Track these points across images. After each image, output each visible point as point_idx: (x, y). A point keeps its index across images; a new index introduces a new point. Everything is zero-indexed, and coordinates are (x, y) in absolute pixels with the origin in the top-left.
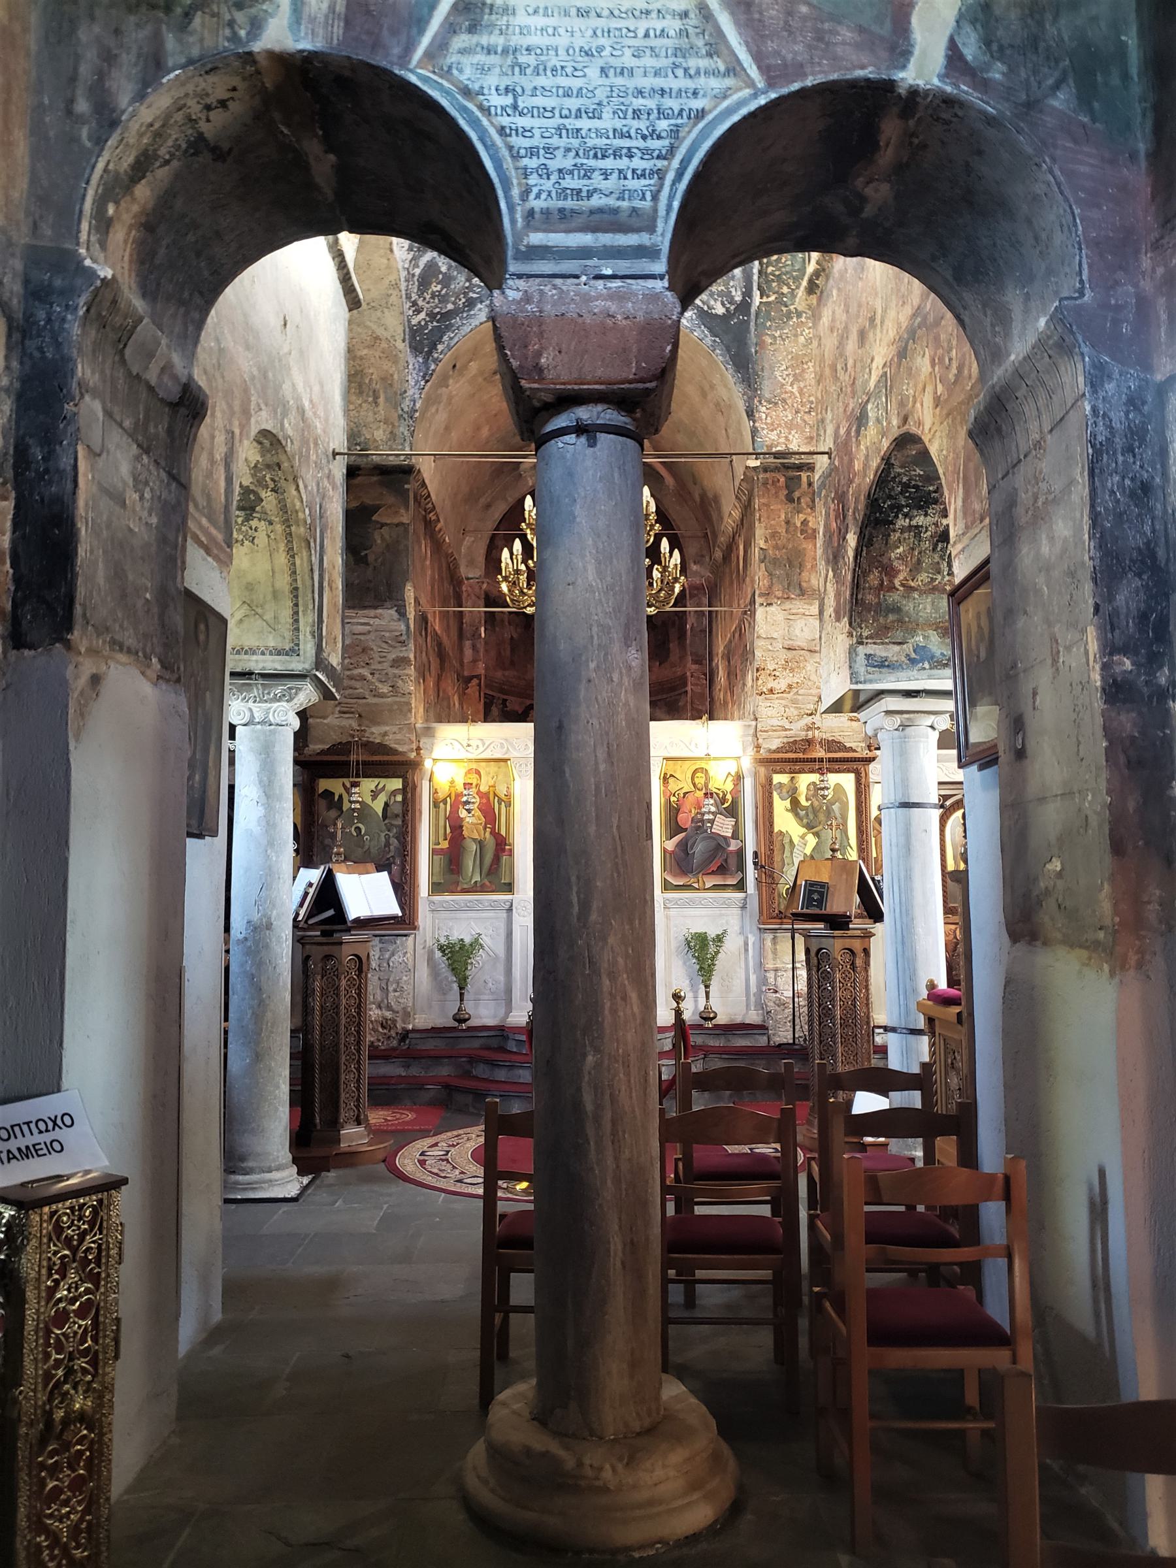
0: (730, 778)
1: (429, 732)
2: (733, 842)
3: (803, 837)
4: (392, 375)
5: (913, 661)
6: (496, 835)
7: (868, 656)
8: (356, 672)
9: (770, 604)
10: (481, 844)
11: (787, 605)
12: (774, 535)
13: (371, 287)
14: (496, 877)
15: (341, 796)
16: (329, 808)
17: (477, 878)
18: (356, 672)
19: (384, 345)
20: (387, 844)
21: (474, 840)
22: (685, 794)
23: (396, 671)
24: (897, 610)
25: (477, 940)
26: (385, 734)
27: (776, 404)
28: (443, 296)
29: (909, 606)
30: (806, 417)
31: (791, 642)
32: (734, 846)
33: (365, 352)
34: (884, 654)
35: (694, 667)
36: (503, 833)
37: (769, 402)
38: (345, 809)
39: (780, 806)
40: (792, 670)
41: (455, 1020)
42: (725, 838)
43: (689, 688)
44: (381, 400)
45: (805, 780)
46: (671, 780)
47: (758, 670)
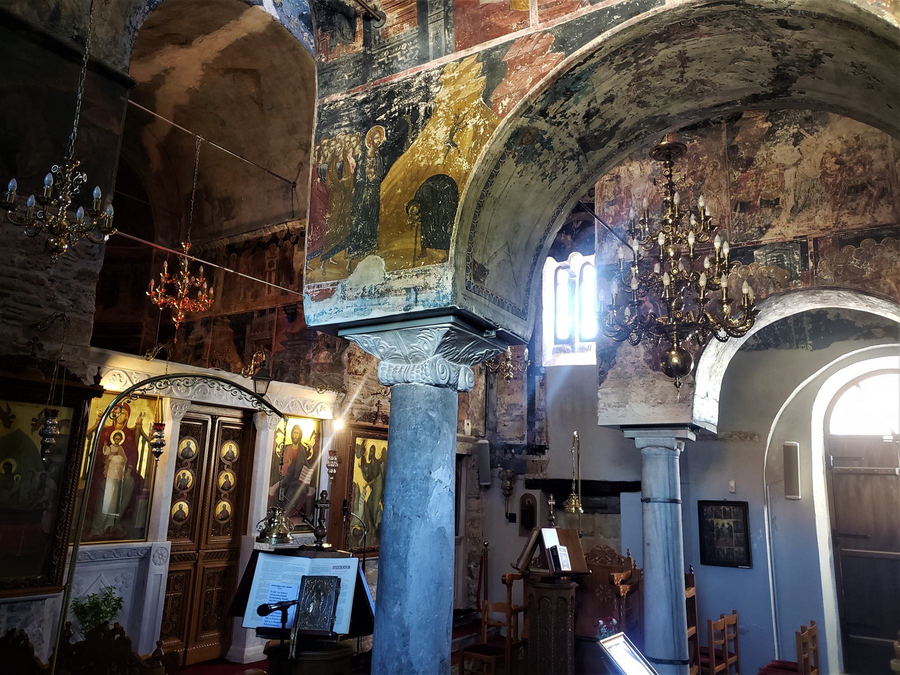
8: (33, 273)
18: (33, 273)
23: (80, 284)
26: (58, 352)
47: (349, 355)
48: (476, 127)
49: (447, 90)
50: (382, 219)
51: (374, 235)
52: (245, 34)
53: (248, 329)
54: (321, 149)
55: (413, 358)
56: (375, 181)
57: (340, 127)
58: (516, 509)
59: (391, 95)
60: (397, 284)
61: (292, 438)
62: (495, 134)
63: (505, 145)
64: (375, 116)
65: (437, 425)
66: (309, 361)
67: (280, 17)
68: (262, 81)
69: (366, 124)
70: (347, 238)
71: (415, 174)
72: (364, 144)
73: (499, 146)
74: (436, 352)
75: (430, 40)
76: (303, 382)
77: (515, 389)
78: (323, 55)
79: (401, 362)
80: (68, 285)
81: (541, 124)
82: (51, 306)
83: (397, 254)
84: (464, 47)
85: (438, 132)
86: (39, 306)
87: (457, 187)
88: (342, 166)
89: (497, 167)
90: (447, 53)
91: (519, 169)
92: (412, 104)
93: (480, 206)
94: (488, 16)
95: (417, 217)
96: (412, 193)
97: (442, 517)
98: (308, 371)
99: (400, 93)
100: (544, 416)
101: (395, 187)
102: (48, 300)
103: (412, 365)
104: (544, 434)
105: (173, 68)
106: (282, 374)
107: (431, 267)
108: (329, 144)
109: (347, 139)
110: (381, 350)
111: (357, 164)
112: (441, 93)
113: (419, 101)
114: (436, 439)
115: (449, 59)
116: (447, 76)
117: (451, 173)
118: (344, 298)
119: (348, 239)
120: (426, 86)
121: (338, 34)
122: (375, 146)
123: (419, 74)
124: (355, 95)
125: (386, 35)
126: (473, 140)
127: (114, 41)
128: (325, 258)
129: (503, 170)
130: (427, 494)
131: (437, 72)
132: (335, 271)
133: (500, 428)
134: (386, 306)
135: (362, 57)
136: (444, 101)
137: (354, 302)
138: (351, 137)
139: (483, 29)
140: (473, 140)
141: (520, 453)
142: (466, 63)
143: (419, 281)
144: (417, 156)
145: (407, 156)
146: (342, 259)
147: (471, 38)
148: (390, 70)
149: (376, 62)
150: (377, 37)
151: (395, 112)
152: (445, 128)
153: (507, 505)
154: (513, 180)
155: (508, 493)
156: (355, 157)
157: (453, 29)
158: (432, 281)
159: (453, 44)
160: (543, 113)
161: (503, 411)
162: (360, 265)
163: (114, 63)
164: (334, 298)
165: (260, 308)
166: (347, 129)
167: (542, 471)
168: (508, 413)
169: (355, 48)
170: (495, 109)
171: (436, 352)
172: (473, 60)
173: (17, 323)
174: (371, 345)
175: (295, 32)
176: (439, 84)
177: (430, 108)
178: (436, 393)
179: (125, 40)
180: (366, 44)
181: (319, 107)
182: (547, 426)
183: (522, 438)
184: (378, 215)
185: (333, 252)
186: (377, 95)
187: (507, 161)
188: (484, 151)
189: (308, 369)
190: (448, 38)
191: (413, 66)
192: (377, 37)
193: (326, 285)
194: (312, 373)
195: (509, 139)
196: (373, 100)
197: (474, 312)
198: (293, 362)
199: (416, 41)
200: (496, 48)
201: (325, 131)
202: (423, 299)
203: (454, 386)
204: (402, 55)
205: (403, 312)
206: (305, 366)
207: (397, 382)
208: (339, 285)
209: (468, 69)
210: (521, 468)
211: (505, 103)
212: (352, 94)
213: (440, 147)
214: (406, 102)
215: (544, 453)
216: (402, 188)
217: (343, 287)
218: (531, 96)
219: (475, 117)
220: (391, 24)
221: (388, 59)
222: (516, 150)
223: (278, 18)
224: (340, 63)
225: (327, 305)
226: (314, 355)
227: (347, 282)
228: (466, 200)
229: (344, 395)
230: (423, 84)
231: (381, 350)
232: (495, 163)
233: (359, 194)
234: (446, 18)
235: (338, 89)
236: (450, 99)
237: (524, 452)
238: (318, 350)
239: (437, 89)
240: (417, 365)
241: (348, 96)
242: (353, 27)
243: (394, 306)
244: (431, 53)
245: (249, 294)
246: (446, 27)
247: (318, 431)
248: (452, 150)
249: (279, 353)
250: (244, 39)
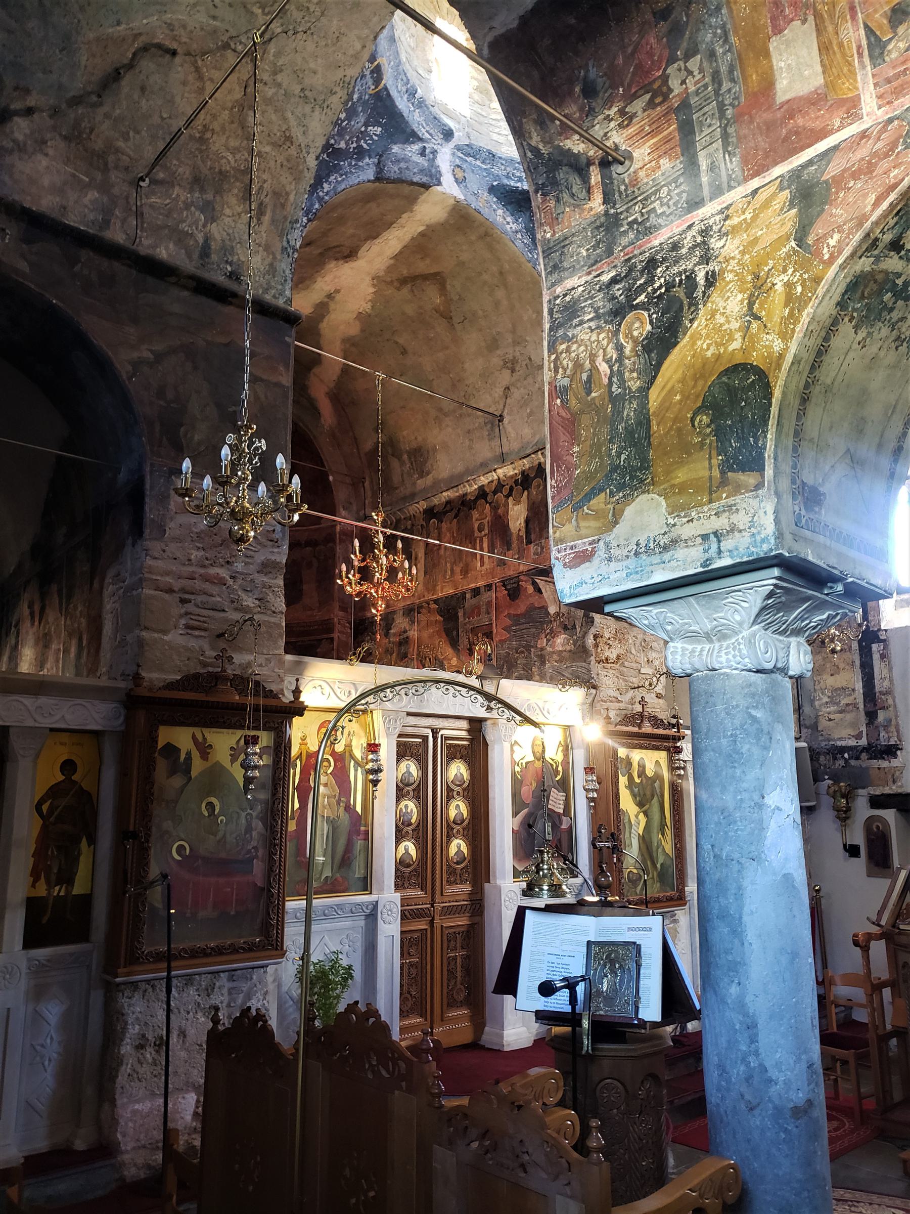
0: (561, 749)
1: (298, 670)
2: (564, 818)
4: (288, 194)
8: (213, 571)
13: (320, 69)
15: (189, 754)
16: (172, 772)
18: (213, 571)
19: (293, 151)
20: (249, 829)
22: (527, 763)
26: (249, 665)
28: (345, 129)
33: (268, 149)
35: (341, 614)
38: (194, 774)
42: (559, 814)
43: (336, 635)
44: (266, 219)
46: (516, 748)
47: (596, 637)
48: (789, 285)
49: (737, 242)
50: (655, 441)
51: (645, 464)
52: (422, 228)
53: (460, 614)
54: (557, 358)
55: (718, 635)
56: (640, 389)
57: (581, 323)
58: (858, 838)
59: (652, 264)
60: (687, 531)
61: (534, 753)
62: (821, 291)
63: (838, 304)
64: (630, 299)
65: (766, 729)
66: (542, 649)
67: (465, 196)
68: (448, 287)
69: (618, 313)
70: (606, 476)
71: (699, 370)
72: (618, 340)
73: (829, 308)
74: (754, 622)
75: (703, 174)
76: (537, 677)
77: (841, 666)
78: (547, 228)
79: (699, 642)
80: (252, 581)
81: (893, 263)
82: (236, 609)
83: (683, 488)
84: (757, 174)
85: (728, 304)
86: (224, 611)
87: (767, 377)
88: (590, 378)
89: (826, 339)
90: (730, 188)
91: (860, 337)
92: (685, 271)
93: (805, 400)
94: (792, 117)
95: (708, 430)
96: (698, 396)
97: (786, 859)
98: (543, 663)
99: (664, 259)
100: (890, 701)
101: (672, 392)
102: (233, 602)
103: (717, 645)
104: (893, 729)
105: (337, 291)
106: (509, 670)
107: (738, 499)
108: (568, 350)
109: (594, 337)
110: (669, 628)
111: (611, 370)
112: (727, 248)
113: (695, 265)
114: (766, 748)
115: (736, 195)
116: (735, 221)
117: (755, 358)
118: (610, 559)
119: (608, 477)
120: (704, 242)
121: (566, 196)
122: (635, 341)
123: (690, 227)
124: (599, 275)
125: (635, 182)
126: (786, 306)
127: (272, 269)
128: (577, 508)
129: (836, 342)
130: (761, 827)
131: (717, 218)
132: (593, 524)
133: (823, 724)
134: (674, 563)
135: (603, 219)
136: (733, 258)
137: (625, 563)
138: (599, 334)
139: (786, 139)
140: (786, 306)
141: (858, 758)
142: (762, 196)
143: (721, 523)
144: (699, 343)
145: (685, 346)
146: (602, 506)
147: (767, 157)
148: (645, 229)
149: (625, 222)
150: (623, 188)
151: (660, 287)
152: (740, 297)
153: (843, 834)
154: (851, 355)
155: (844, 816)
156: (608, 361)
157: (737, 151)
158: (741, 519)
159: (739, 173)
160: (896, 246)
161: (825, 699)
162: (629, 511)
163: (274, 297)
164: (596, 560)
165: (473, 585)
166: (593, 324)
167: (894, 782)
168: (833, 701)
169: (591, 209)
170: (818, 253)
171: (754, 622)
172: (773, 188)
173: (202, 633)
174: (653, 621)
175: (486, 212)
176: (722, 235)
177: (713, 272)
178: (759, 682)
179: (283, 266)
180: (607, 199)
181: (550, 301)
182: (897, 716)
183: (859, 737)
184: (648, 436)
185: (588, 497)
186: (631, 270)
187: (841, 327)
188: (805, 318)
189: (542, 660)
190: (732, 165)
191: (680, 216)
192: (623, 188)
193: (582, 544)
194: (548, 665)
195: (843, 295)
196: (626, 276)
197: (810, 558)
198: (522, 652)
199: (681, 180)
200: (810, 162)
201: (561, 332)
202: (729, 547)
203: (784, 670)
204: (662, 205)
205: (701, 570)
206: (537, 656)
207: (697, 671)
208: (601, 543)
209: (767, 204)
210: (860, 780)
211: (832, 242)
212: (594, 274)
213: (735, 325)
214: (676, 269)
215: (895, 756)
216: (682, 393)
217: (607, 545)
218: (876, 223)
219: (785, 271)
220: (640, 164)
221: (642, 215)
222: (854, 310)
223: (463, 198)
224: (573, 235)
225: (586, 571)
226: (548, 640)
227: (613, 536)
228: (784, 394)
229: (594, 691)
230: (699, 239)
231: (669, 628)
232: (823, 334)
233: (617, 412)
234: (725, 136)
235: (573, 270)
236: (743, 253)
237: (864, 756)
238: (553, 634)
239: (720, 244)
240: (725, 644)
241: (589, 278)
242: (585, 179)
243: (686, 561)
244: (706, 192)
245: (457, 569)
246: (725, 150)
247: (566, 741)
248: (755, 325)
249: (502, 642)
250: (422, 234)
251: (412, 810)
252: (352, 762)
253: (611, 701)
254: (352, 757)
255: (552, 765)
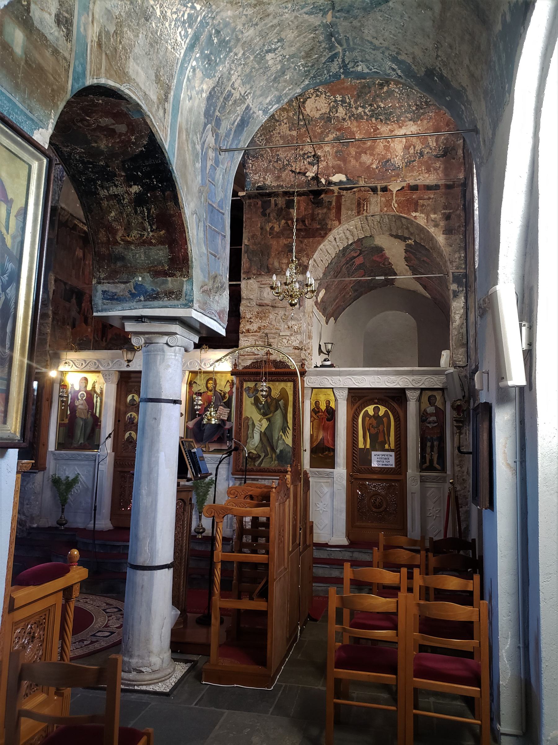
0: (228, 384)
2: (228, 423)
3: (260, 421)
5: (133, 296)
6: (93, 415)
7: (104, 292)
9: (249, 278)
10: (85, 421)
11: (260, 279)
12: (253, 237)
14: (92, 440)
17: (82, 441)
21: (82, 419)
24: (122, 258)
25: (77, 477)
27: (258, 157)
29: (129, 256)
30: (275, 165)
31: (261, 301)
32: (227, 427)
34: (114, 291)
36: (97, 415)
37: (253, 157)
39: (248, 402)
40: (261, 318)
41: (58, 523)
45: (264, 385)
46: (194, 385)
251: (134, 417)
252: (95, 395)
253: (249, 355)
254: (95, 392)
255: (220, 394)
